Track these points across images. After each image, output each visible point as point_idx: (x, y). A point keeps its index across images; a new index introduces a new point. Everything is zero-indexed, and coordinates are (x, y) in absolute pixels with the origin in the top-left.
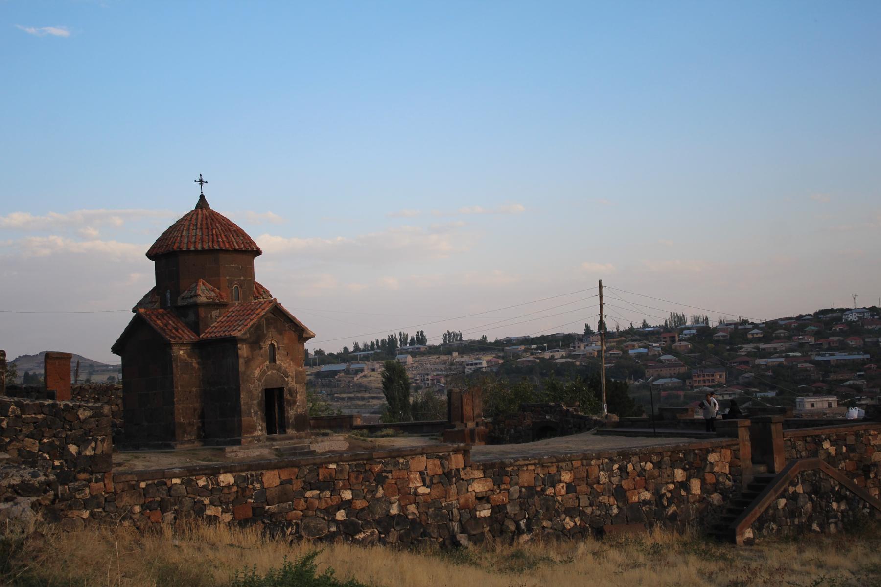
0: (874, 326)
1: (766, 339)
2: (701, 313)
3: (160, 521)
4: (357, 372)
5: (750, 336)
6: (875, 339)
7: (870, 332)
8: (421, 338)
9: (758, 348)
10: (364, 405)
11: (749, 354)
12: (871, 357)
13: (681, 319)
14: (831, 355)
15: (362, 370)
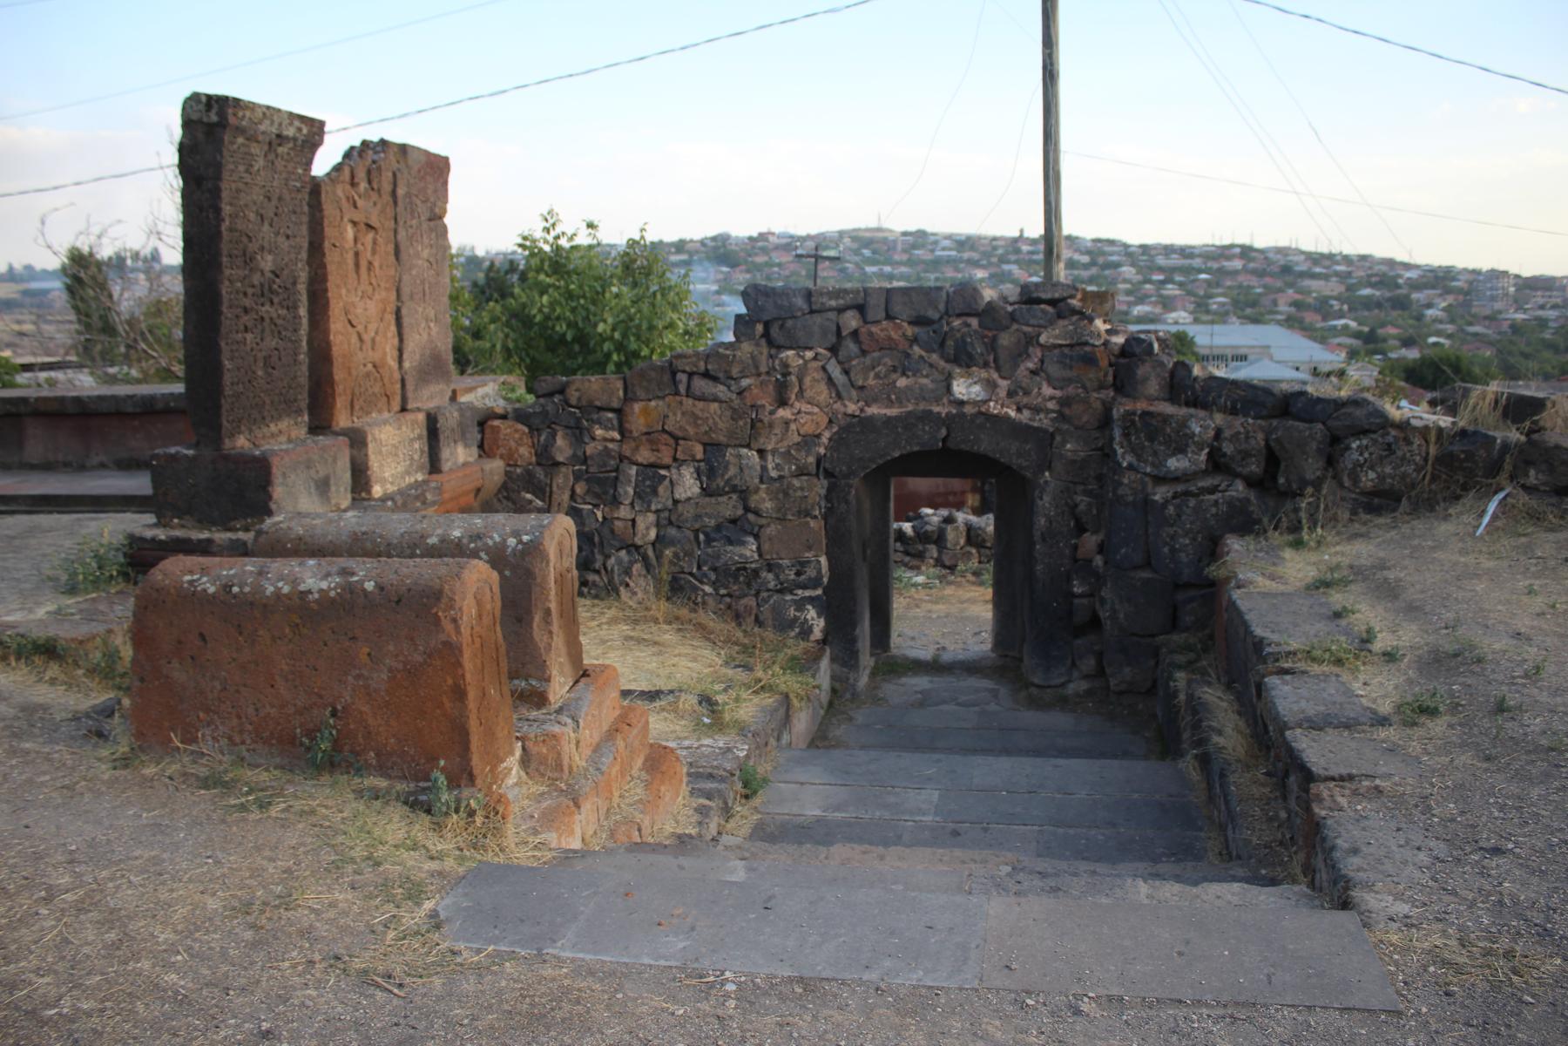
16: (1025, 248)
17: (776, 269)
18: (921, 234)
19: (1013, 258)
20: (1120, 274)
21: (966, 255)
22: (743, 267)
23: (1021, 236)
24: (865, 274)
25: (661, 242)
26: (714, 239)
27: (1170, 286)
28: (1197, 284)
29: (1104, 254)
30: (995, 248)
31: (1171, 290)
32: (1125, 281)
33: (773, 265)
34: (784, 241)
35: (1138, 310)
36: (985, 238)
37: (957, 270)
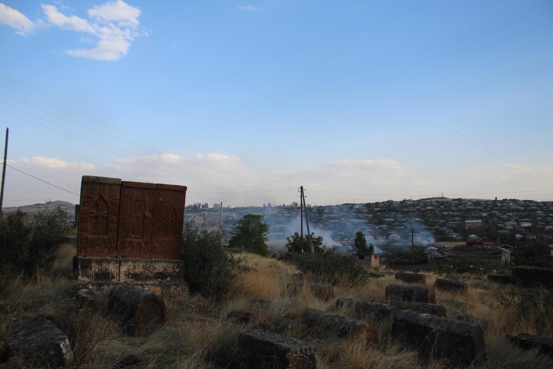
0: (365, 211)
3: (292, 307)
5: (324, 212)
6: (367, 215)
7: (364, 212)
8: (206, 205)
9: (329, 216)
11: (326, 218)
14: (355, 220)
15: (191, 216)
18: (460, 200)
19: (495, 208)
20: (537, 214)
21: (478, 208)
24: (443, 214)
25: (370, 203)
26: (388, 202)
29: (529, 206)
30: (488, 205)
32: (539, 216)
35: (548, 227)
36: (483, 201)
37: (476, 213)
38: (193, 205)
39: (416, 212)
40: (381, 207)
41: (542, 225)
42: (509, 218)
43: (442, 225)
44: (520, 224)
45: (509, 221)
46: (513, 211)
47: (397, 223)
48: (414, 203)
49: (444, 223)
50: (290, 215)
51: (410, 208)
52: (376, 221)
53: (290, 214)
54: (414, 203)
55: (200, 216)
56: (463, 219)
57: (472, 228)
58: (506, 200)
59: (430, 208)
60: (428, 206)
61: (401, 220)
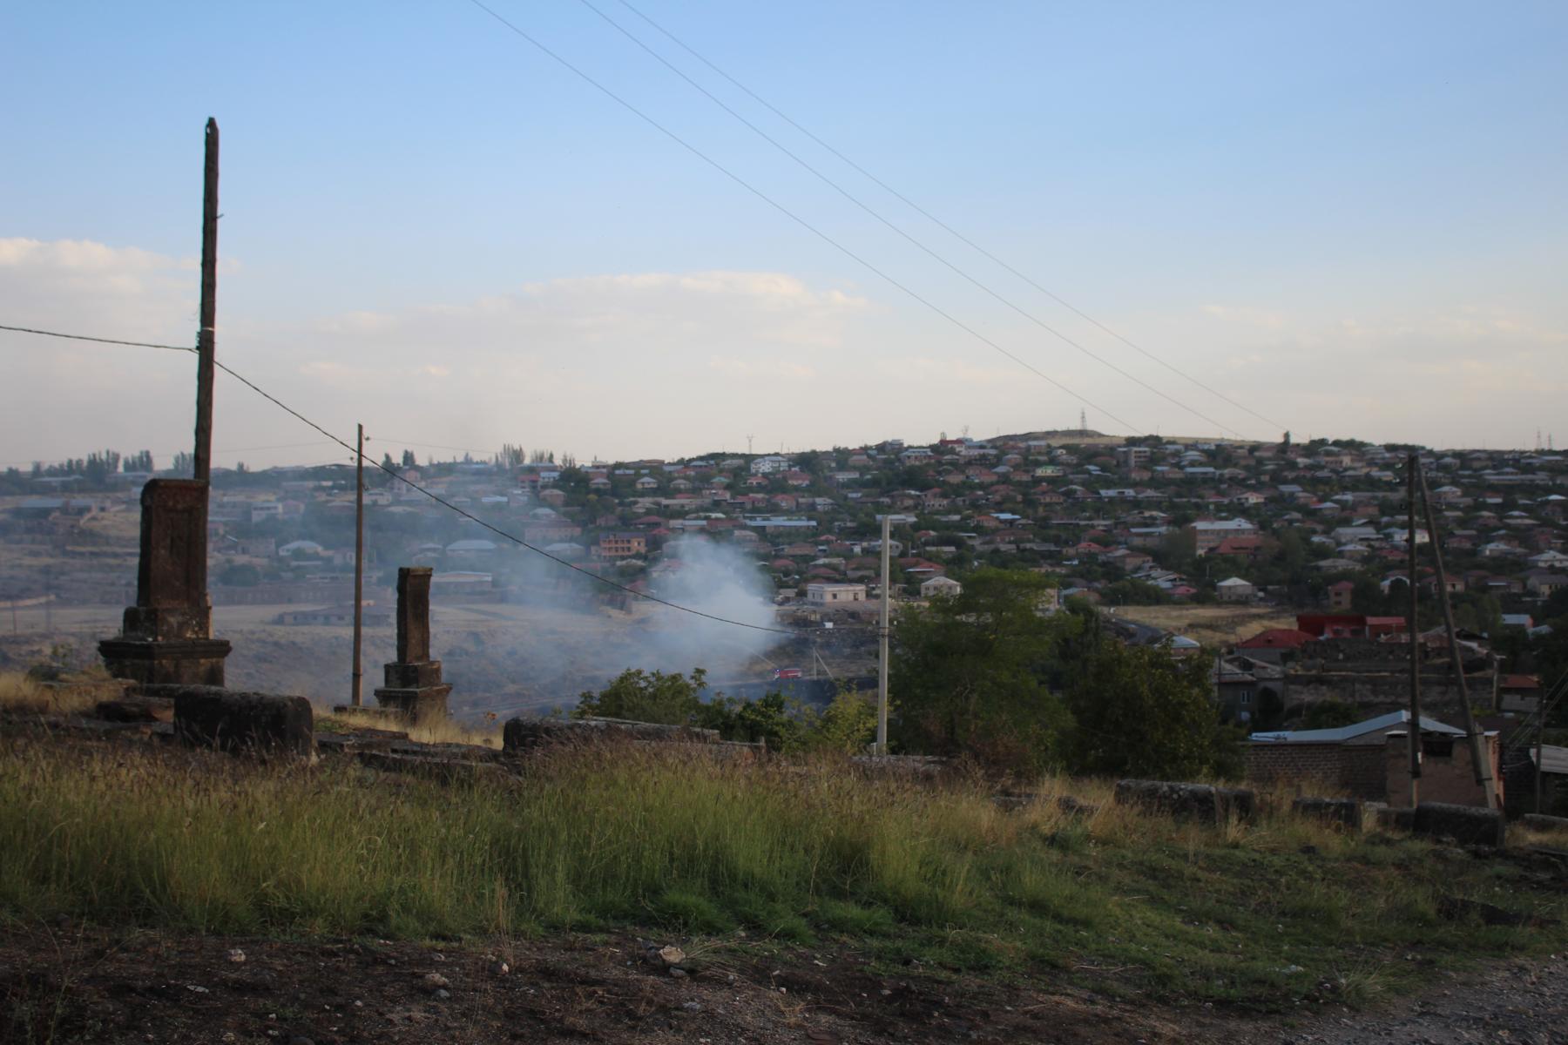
0: (800, 482)
1: (664, 489)
2: (545, 447)
4: (81, 511)
5: (639, 486)
6: (810, 500)
7: (797, 488)
9: (659, 504)
10: (119, 566)
11: (649, 512)
12: (818, 524)
13: (518, 455)
15: (88, 509)
16: (1302, 461)
17: (980, 493)
18: (1154, 441)
19: (1290, 475)
20: (1439, 496)
21: (1227, 472)
22: (937, 490)
23: (1286, 442)
24: (1101, 498)
25: (814, 452)
26: (882, 448)
27: (1516, 513)
28: (1549, 509)
30: (1260, 462)
31: (1518, 518)
32: (1452, 506)
33: (973, 487)
34: (976, 452)
35: (1491, 549)
36: (1241, 447)
38: (85, 460)
39: (996, 487)
40: (863, 469)
41: (1469, 538)
42: (1346, 513)
43: (1106, 542)
44: (1388, 537)
45: (1347, 522)
46: (1355, 484)
47: (932, 533)
48: (982, 451)
49: (1108, 530)
50: (505, 499)
51: (970, 472)
52: (849, 524)
53: (502, 495)
54: (982, 451)
55: (123, 507)
56: (1181, 520)
57: (1221, 551)
58: (1323, 442)
59: (1048, 471)
60: (1038, 464)
61: (944, 519)
